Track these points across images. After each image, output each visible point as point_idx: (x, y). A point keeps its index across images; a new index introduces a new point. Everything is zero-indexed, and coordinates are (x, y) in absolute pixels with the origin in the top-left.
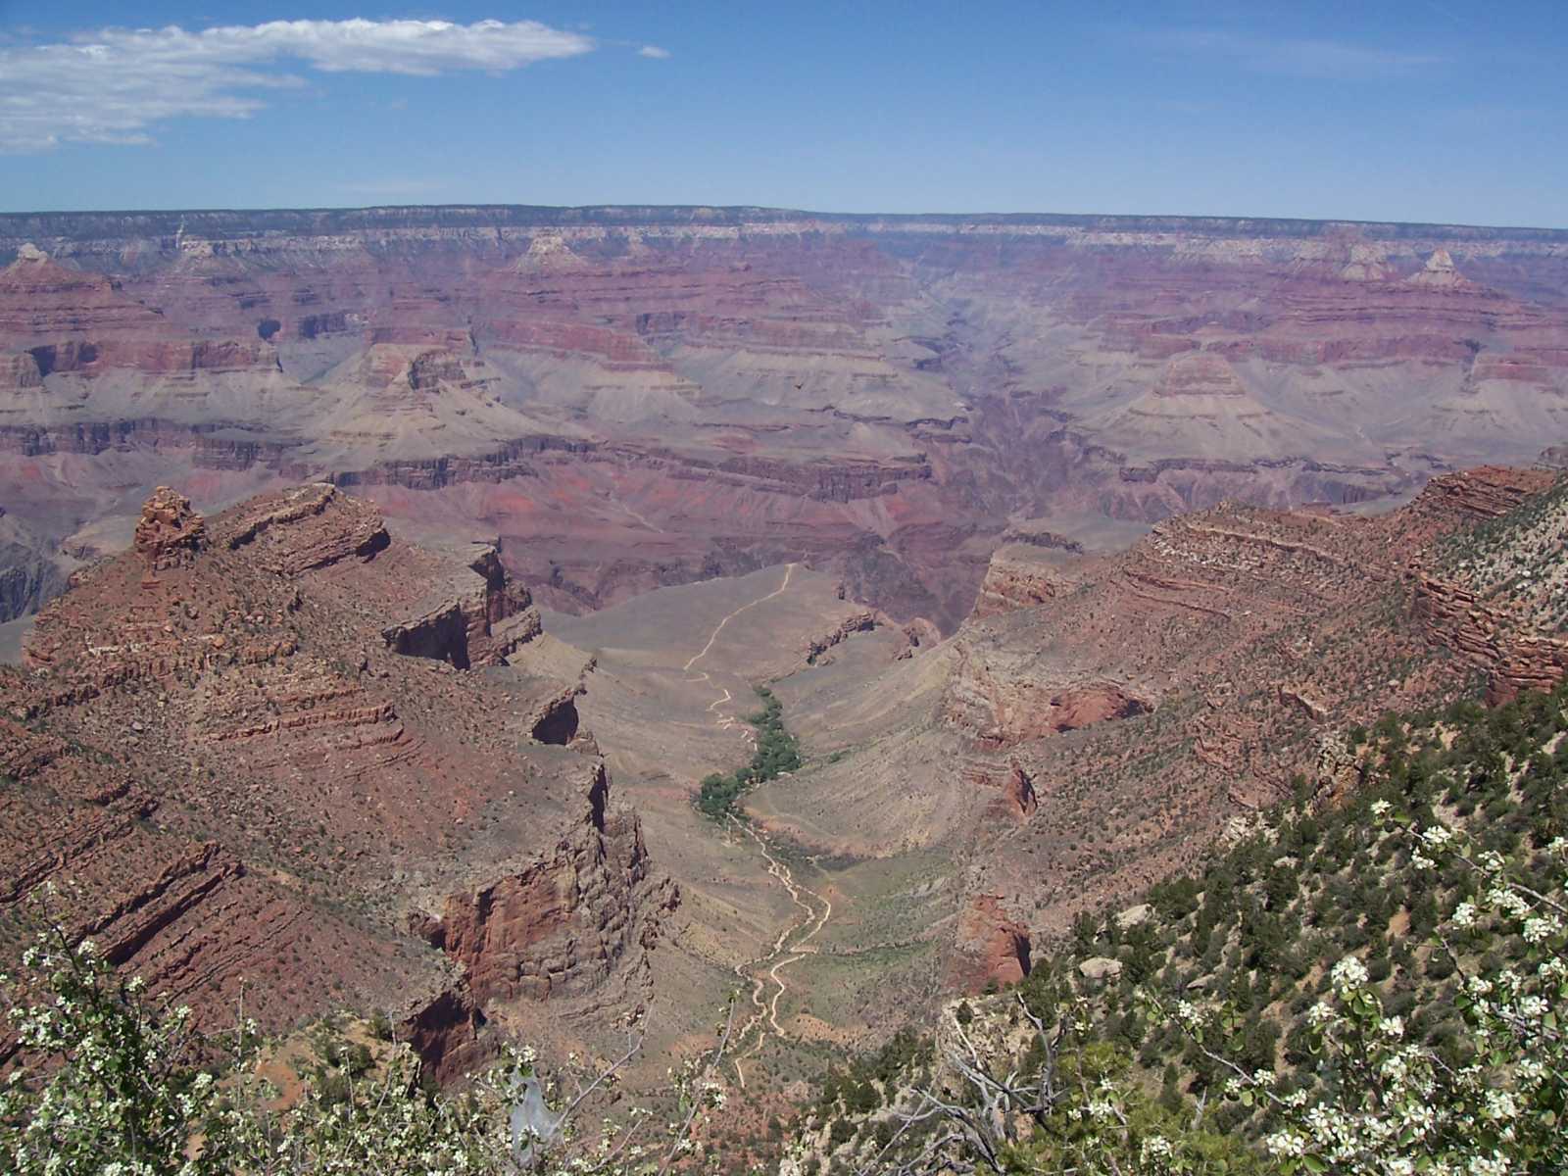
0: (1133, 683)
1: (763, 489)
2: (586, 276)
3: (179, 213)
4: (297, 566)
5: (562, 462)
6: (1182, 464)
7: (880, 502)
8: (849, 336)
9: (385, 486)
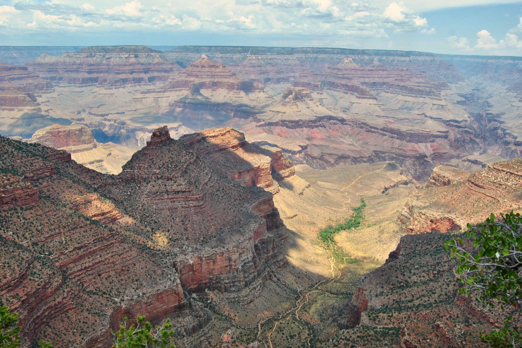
0: (458, 219)
2: (357, 70)
3: (250, 47)
4: (212, 150)
5: (335, 124)
7: (429, 145)
8: (433, 92)
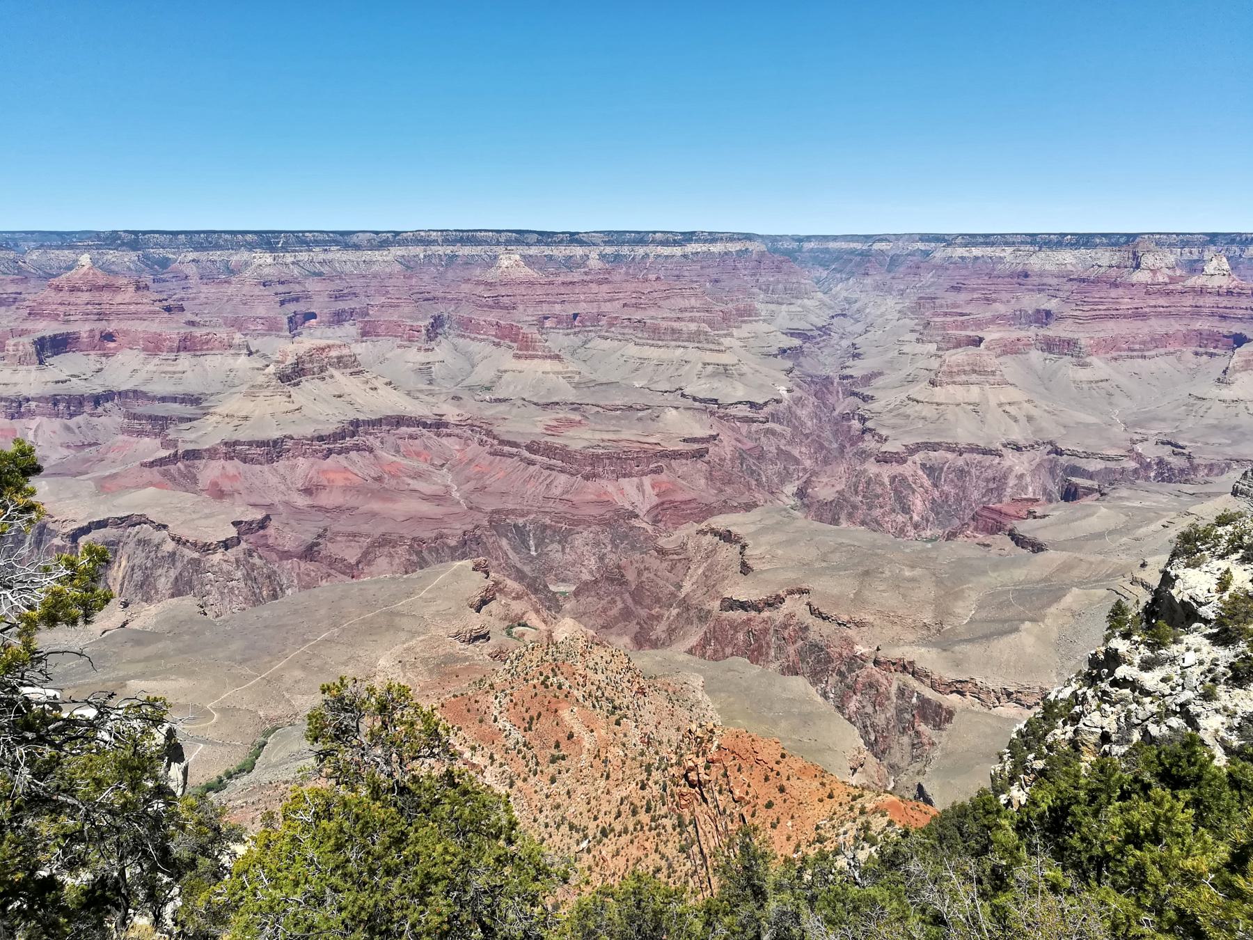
1: (550, 468)
6: (935, 447)
7: (647, 481)
9: (222, 461)
